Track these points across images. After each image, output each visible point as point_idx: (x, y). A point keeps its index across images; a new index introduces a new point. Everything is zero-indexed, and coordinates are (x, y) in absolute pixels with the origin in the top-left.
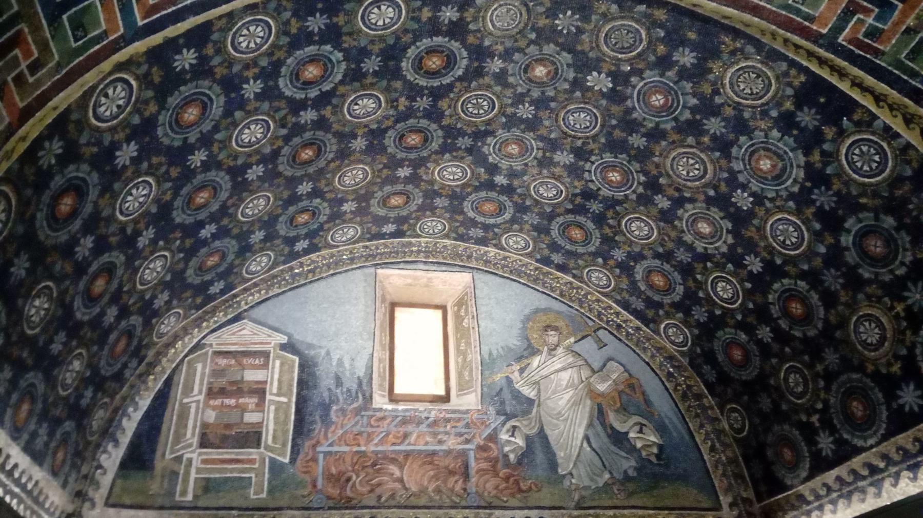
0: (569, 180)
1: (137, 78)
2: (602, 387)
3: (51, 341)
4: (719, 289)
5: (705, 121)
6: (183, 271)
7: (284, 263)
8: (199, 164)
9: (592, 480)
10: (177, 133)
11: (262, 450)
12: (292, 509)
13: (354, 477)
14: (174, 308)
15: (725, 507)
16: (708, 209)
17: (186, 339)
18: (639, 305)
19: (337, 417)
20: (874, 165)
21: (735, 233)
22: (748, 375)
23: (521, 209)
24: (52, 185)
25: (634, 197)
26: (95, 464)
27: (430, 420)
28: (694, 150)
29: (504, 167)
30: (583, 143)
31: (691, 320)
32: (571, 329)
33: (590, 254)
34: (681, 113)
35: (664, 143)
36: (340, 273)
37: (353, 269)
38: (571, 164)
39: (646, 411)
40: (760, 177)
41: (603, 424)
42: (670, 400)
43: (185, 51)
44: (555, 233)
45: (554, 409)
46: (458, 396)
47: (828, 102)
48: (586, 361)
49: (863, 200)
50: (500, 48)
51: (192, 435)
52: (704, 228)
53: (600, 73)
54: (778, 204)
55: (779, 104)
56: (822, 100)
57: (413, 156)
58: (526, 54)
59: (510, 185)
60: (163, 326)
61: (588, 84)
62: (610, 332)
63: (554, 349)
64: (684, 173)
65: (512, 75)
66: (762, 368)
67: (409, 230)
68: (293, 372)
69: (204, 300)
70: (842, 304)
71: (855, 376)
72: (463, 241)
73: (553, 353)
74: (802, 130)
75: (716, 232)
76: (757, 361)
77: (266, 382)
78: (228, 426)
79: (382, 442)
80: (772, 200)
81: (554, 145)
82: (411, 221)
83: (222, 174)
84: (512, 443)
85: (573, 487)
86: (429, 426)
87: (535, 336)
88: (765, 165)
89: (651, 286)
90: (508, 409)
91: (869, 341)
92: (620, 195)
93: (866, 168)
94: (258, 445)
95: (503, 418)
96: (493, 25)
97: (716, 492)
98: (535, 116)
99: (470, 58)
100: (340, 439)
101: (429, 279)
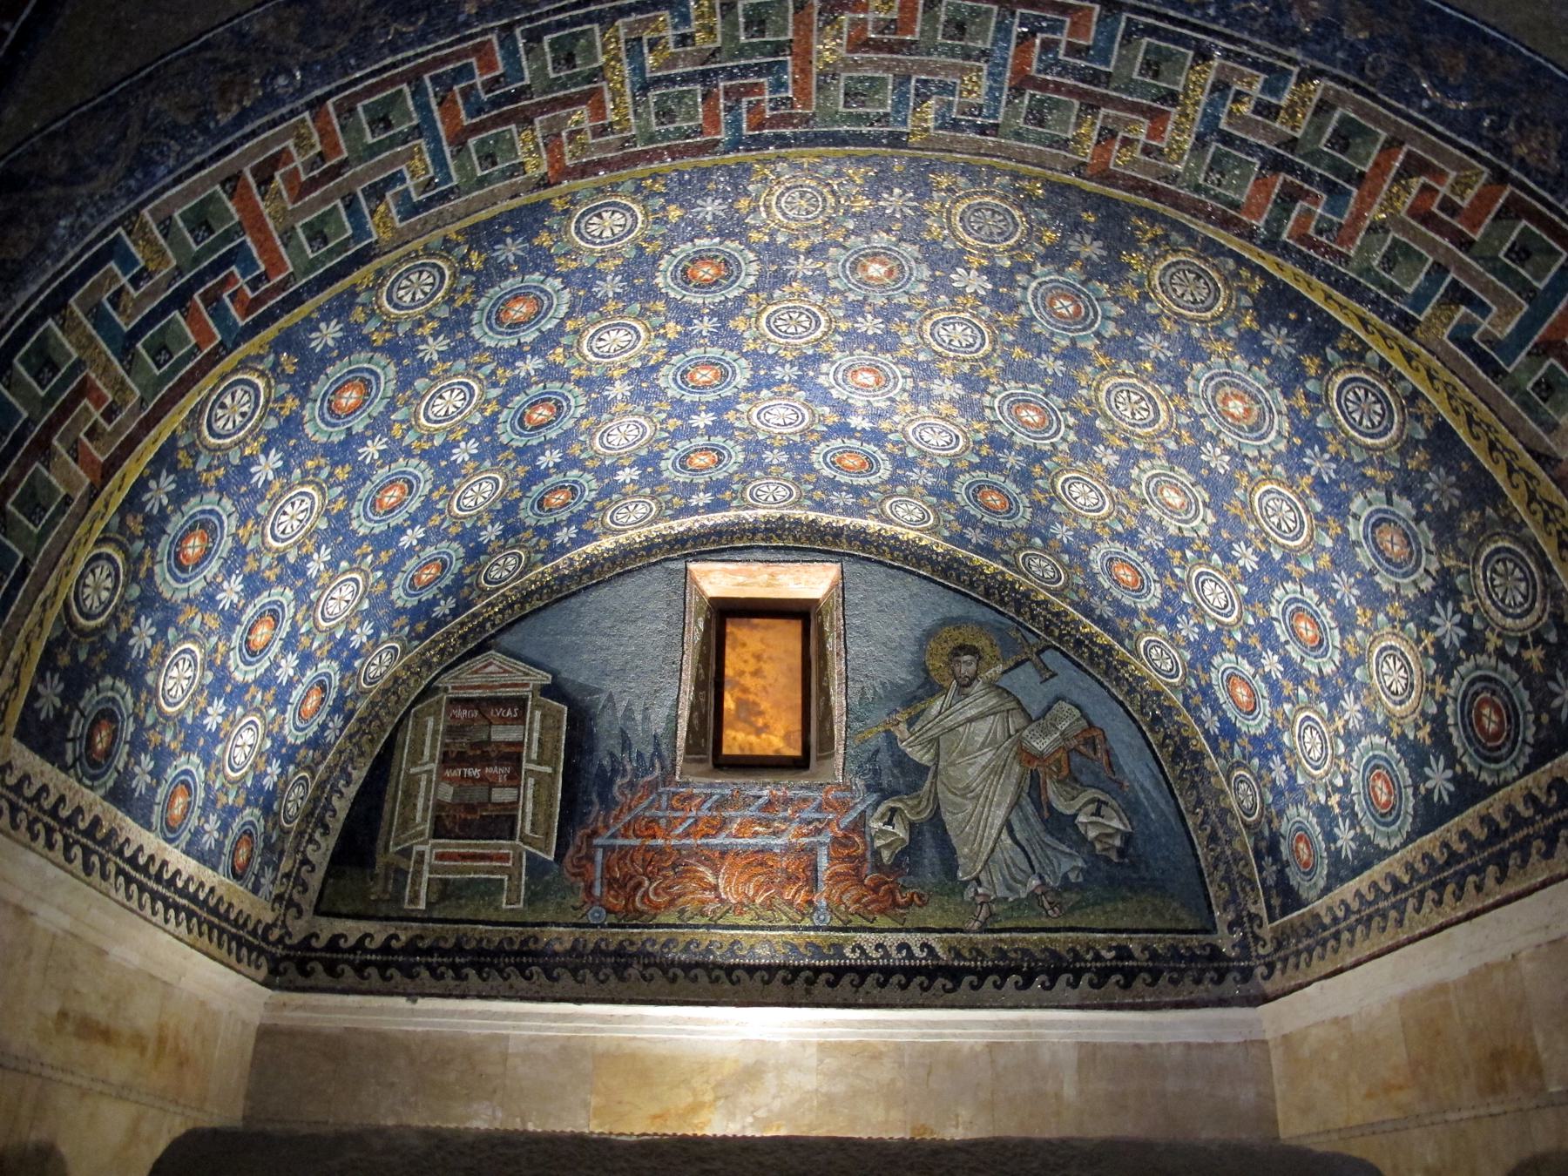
0: (960, 420)
1: (262, 374)
2: (1041, 744)
3: (204, 713)
4: (1207, 592)
6: (388, 592)
9: (1010, 888)
10: (334, 425)
11: (517, 842)
12: (558, 925)
13: (647, 883)
15: (1222, 928)
16: (1172, 469)
17: (412, 682)
19: (623, 794)
20: (1377, 419)
21: (1215, 505)
22: (1257, 726)
23: (902, 462)
24: (170, 529)
25: (1064, 447)
26: (299, 856)
27: (761, 801)
28: (1134, 381)
29: (860, 404)
32: (998, 651)
33: (1023, 530)
35: (1089, 369)
36: (630, 571)
38: (962, 398)
39: (1111, 781)
41: (1038, 805)
42: (1153, 765)
43: (323, 325)
44: (961, 498)
45: (959, 781)
46: (819, 759)
47: (1301, 320)
48: (1019, 702)
49: (1370, 472)
50: (804, 245)
51: (422, 819)
52: (1176, 500)
53: (968, 270)
54: (1264, 467)
55: (1237, 321)
56: (1292, 316)
57: (710, 397)
58: (845, 248)
59: (873, 430)
62: (1062, 653)
63: (968, 685)
64: (1128, 413)
66: (1272, 718)
68: (559, 728)
69: (427, 626)
70: (1360, 627)
71: (1377, 739)
72: (825, 511)
74: (1276, 359)
75: (1190, 503)
76: (1265, 705)
77: (521, 744)
78: (470, 808)
79: (687, 834)
80: (1255, 460)
81: (927, 372)
83: (415, 461)
84: (887, 834)
85: (979, 900)
86: (761, 809)
87: (938, 664)
88: (1236, 407)
89: (1117, 582)
90: (885, 781)
91: (1393, 688)
92: (1045, 445)
93: (1366, 422)
94: (512, 836)
95: (875, 796)
96: (784, 214)
97: (1210, 905)
98: (888, 332)
100: (627, 827)
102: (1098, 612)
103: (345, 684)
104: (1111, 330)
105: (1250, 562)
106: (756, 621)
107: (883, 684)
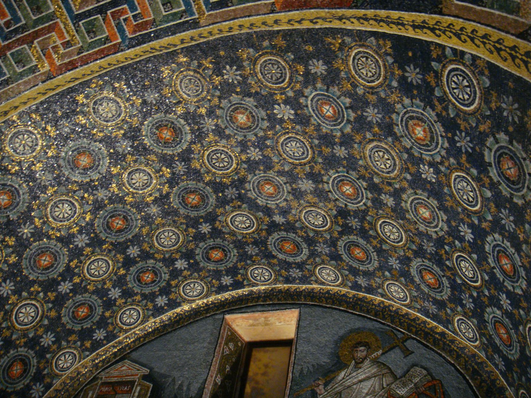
0: (321, 204)
5: (365, 114)
6: (59, 317)
7: (154, 316)
8: (29, 235)
14: (65, 348)
18: (433, 309)
21: (442, 208)
23: (310, 242)
25: (369, 204)
29: (274, 207)
30: (312, 168)
31: (467, 310)
34: (348, 115)
35: (356, 146)
36: (197, 321)
37: (206, 317)
38: (315, 190)
40: (423, 145)
48: (390, 369)
50: (203, 111)
56: (410, 54)
60: (60, 362)
61: (279, 116)
63: (362, 362)
64: (383, 166)
65: (226, 127)
67: (244, 280)
68: (147, 394)
72: (291, 282)
73: (360, 365)
75: (432, 212)
80: (442, 163)
82: (241, 271)
87: (345, 353)
99: (189, 124)
101: (265, 318)
102: (430, 312)
103: (42, 365)
104: (352, 115)
105: (469, 237)
106: (268, 348)
107: (313, 365)
